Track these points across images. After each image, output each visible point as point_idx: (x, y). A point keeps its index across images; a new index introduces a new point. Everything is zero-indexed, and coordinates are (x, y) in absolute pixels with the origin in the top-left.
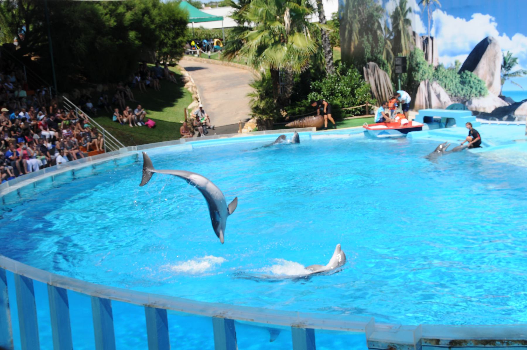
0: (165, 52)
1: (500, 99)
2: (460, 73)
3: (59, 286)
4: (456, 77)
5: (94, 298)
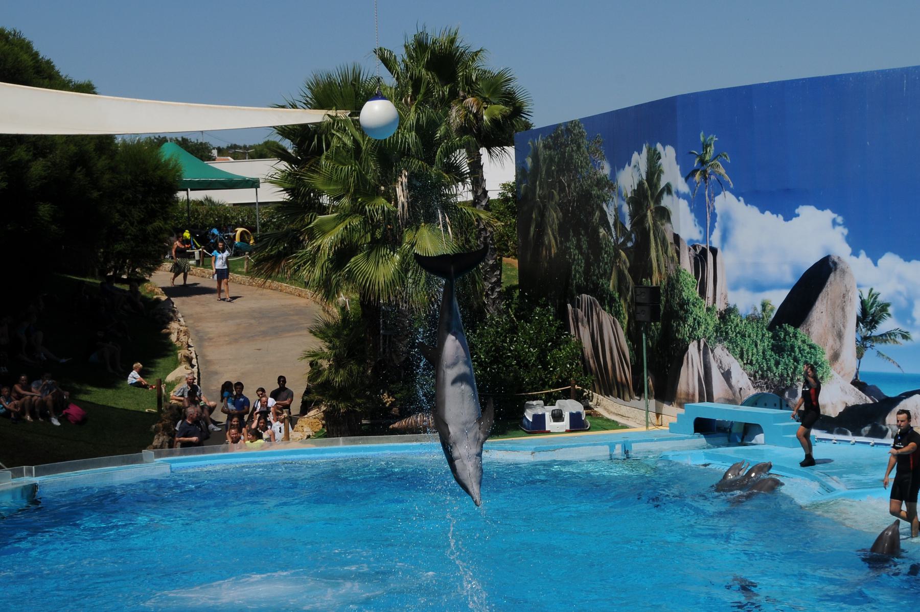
2: (771, 328)
4: (763, 335)
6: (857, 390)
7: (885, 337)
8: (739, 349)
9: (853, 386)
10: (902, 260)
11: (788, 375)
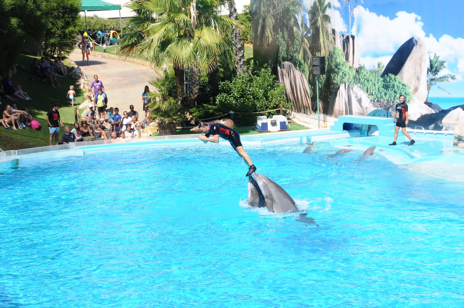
0: (52, 44)
1: (427, 106)
2: (383, 76)
4: (378, 80)
7: (442, 79)
8: (366, 87)
9: (425, 105)
10: (452, 38)
11: (391, 100)
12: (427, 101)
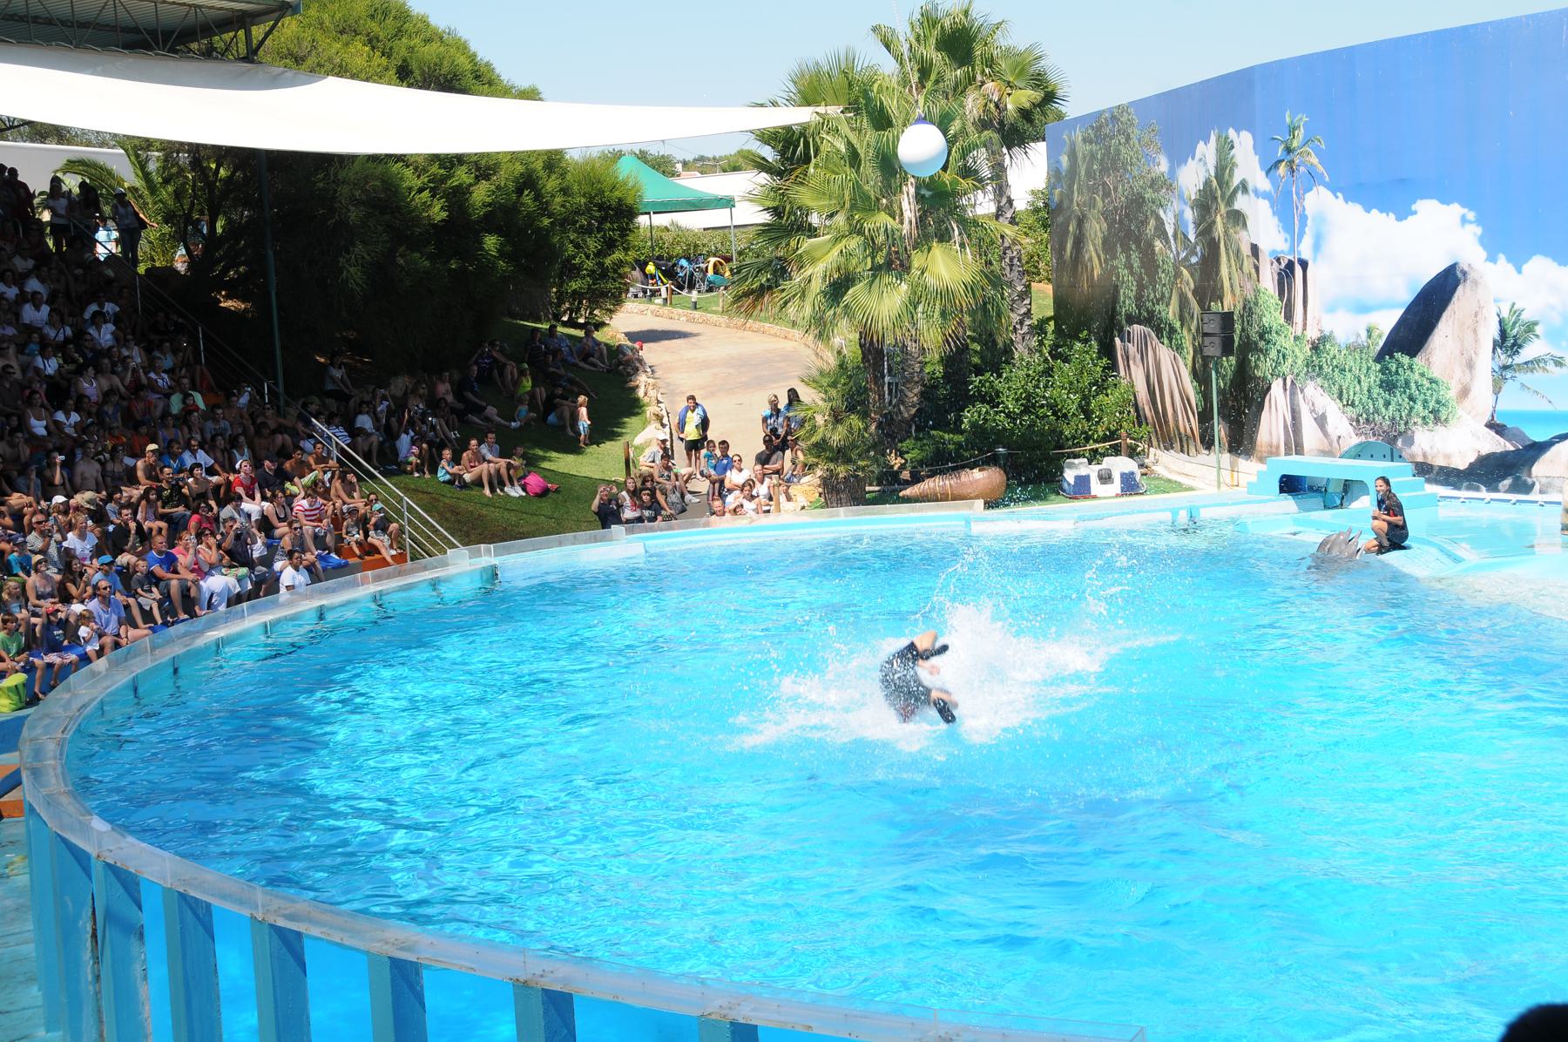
0: (575, 292)
1: (1493, 433)
2: (1379, 358)
3: (281, 923)
4: (1368, 369)
5: (373, 958)
6: (1494, 434)
7: (1531, 365)
8: (1337, 387)
9: (1487, 429)
10: (1555, 264)
11: (1401, 416)
12: (1493, 416)
